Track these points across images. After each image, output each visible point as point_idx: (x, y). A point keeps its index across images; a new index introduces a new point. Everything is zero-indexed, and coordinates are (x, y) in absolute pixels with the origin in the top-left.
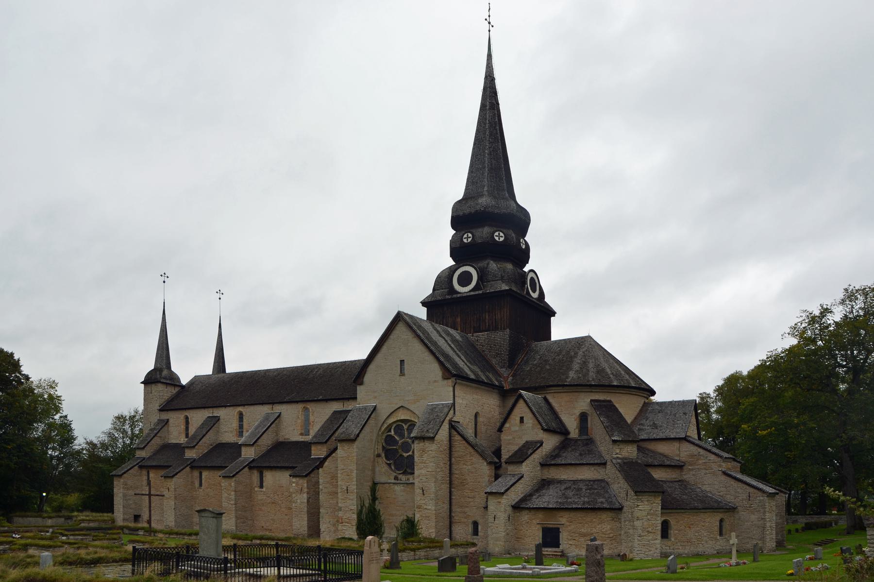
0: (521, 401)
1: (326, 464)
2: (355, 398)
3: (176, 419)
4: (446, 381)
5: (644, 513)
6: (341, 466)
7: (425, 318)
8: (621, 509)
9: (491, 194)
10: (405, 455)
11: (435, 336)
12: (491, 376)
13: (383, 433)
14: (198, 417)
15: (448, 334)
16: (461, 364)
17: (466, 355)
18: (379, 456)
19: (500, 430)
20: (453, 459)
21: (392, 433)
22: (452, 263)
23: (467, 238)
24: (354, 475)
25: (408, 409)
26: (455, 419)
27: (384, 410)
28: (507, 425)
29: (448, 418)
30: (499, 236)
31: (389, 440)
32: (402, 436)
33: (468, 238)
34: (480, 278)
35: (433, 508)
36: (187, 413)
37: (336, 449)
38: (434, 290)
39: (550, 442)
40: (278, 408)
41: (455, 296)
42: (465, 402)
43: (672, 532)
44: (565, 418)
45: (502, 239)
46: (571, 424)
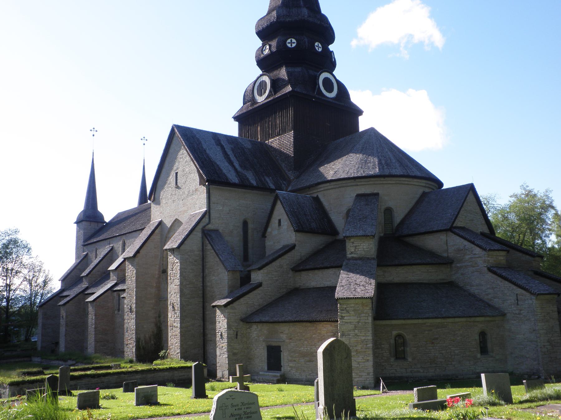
5: (351, 327)
19: (264, 235)
26: (210, 227)
28: (269, 230)
45: (294, 45)
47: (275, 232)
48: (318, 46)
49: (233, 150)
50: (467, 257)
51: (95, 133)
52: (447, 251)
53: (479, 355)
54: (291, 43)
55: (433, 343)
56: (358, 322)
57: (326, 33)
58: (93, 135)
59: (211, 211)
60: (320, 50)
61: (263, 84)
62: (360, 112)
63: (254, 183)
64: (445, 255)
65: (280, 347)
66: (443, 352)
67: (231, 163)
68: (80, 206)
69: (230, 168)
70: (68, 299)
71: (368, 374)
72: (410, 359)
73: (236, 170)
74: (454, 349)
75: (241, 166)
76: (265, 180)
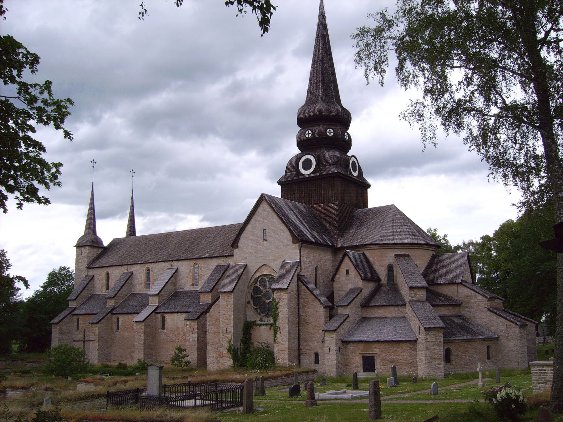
0: (347, 258)
1: (212, 310)
2: (233, 255)
4: (294, 245)
5: (431, 344)
6: (222, 312)
7: (280, 196)
8: (416, 341)
9: (324, 101)
10: (267, 301)
11: (287, 211)
12: (325, 238)
13: (251, 285)
14: (116, 274)
15: (296, 207)
16: (305, 231)
17: (308, 223)
18: (249, 302)
19: (333, 280)
20: (300, 304)
21: (258, 285)
22: (297, 151)
23: (309, 134)
24: (232, 318)
25: (269, 267)
27: (252, 268)
28: (337, 276)
29: (296, 273)
30: (330, 132)
31: (256, 290)
32: (265, 286)
33: (309, 134)
34: (318, 164)
35: (287, 343)
36: (108, 270)
37: (219, 297)
38: (286, 172)
39: (368, 288)
40: (176, 264)
41: (300, 177)
42: (308, 260)
43: (453, 357)
44: (377, 269)
45: (332, 134)
46: (382, 273)
47: (342, 279)
50: (473, 301)
51: (95, 165)
52: (457, 296)
53: (487, 360)
64: (456, 298)
67: (304, 225)
68: (80, 230)
71: (441, 372)
72: (454, 363)
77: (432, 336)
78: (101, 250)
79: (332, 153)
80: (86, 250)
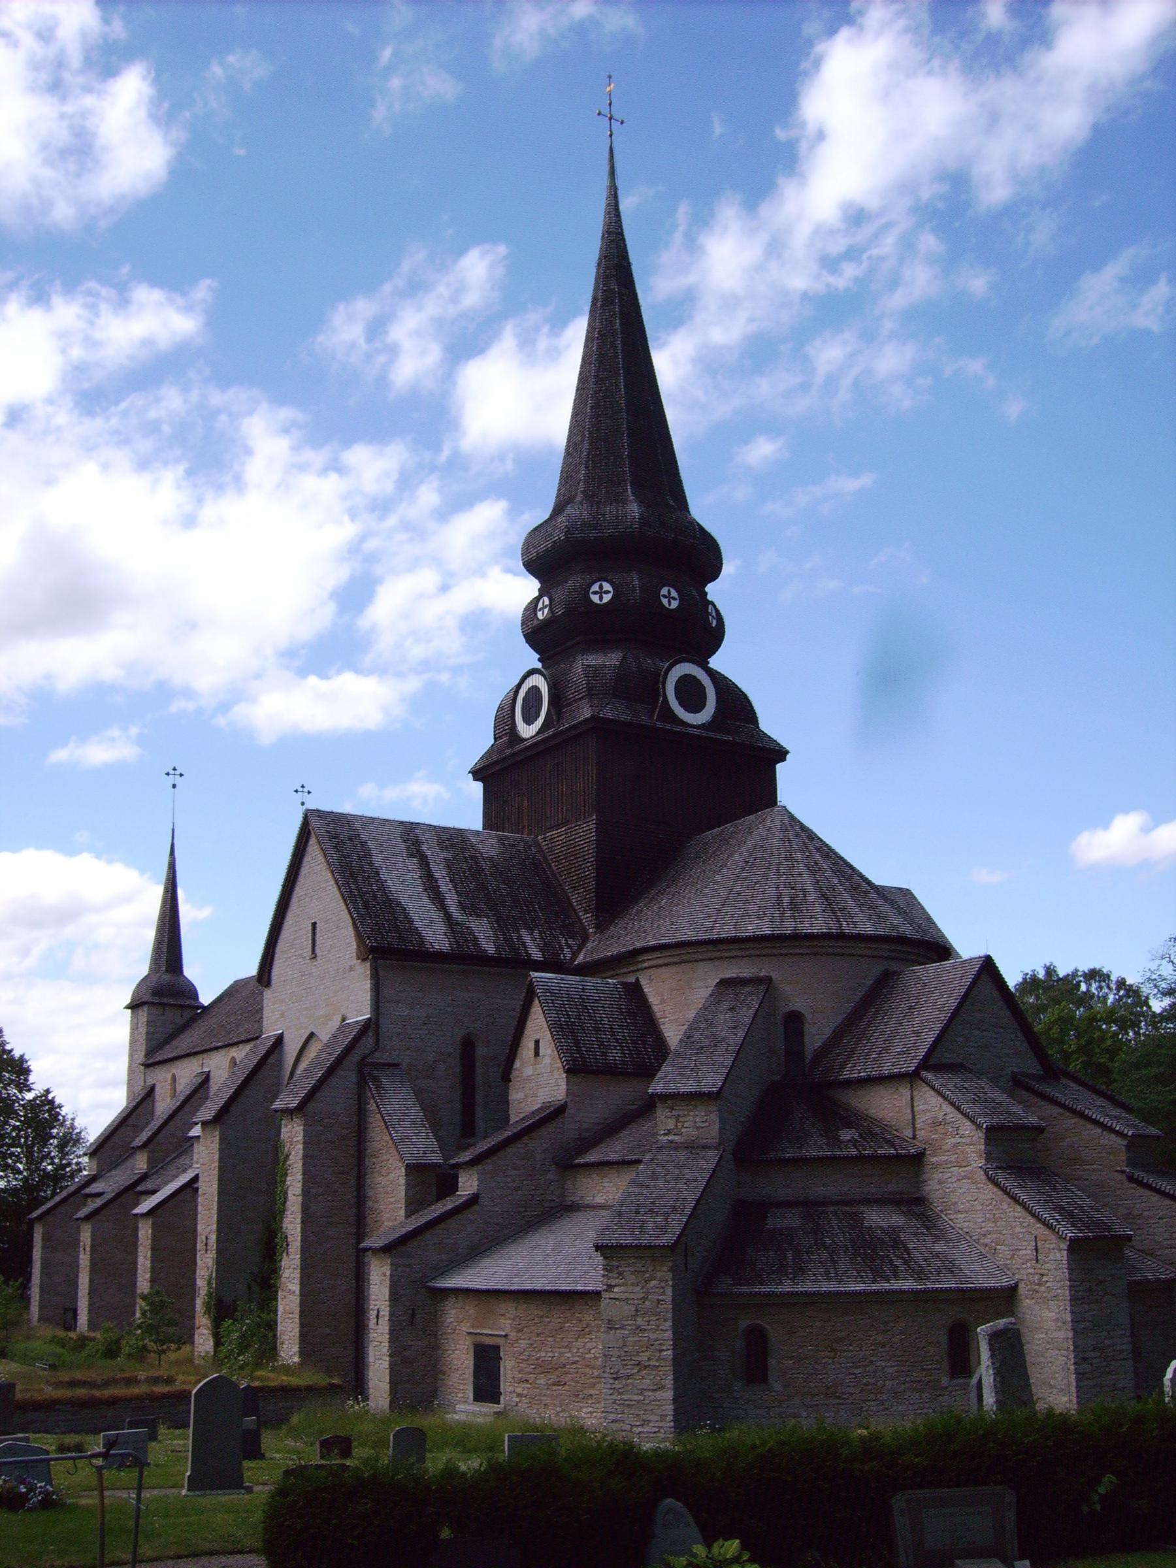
3: (161, 1078)
5: (628, 1310)
26: (380, 1057)
28: (517, 1064)
29: (356, 1056)
30: (601, 592)
45: (607, 598)
47: (528, 1071)
48: (668, 596)
49: (449, 865)
53: (945, 1380)
54: (601, 592)
55: (833, 1350)
56: (644, 1299)
57: (700, 557)
58: (174, 786)
59: (381, 1021)
60: (675, 604)
61: (535, 691)
62: (781, 754)
63: (490, 949)
65: (497, 1348)
66: (858, 1371)
68: (137, 965)
69: (435, 915)
70: (99, 1202)
71: (663, 1417)
72: (778, 1387)
73: (448, 916)
74: (883, 1364)
75: (462, 906)
76: (520, 938)
77: (632, 1278)
78: (188, 1014)
79: (594, 659)
80: (143, 1015)
